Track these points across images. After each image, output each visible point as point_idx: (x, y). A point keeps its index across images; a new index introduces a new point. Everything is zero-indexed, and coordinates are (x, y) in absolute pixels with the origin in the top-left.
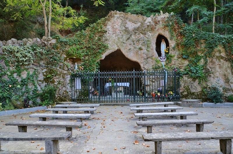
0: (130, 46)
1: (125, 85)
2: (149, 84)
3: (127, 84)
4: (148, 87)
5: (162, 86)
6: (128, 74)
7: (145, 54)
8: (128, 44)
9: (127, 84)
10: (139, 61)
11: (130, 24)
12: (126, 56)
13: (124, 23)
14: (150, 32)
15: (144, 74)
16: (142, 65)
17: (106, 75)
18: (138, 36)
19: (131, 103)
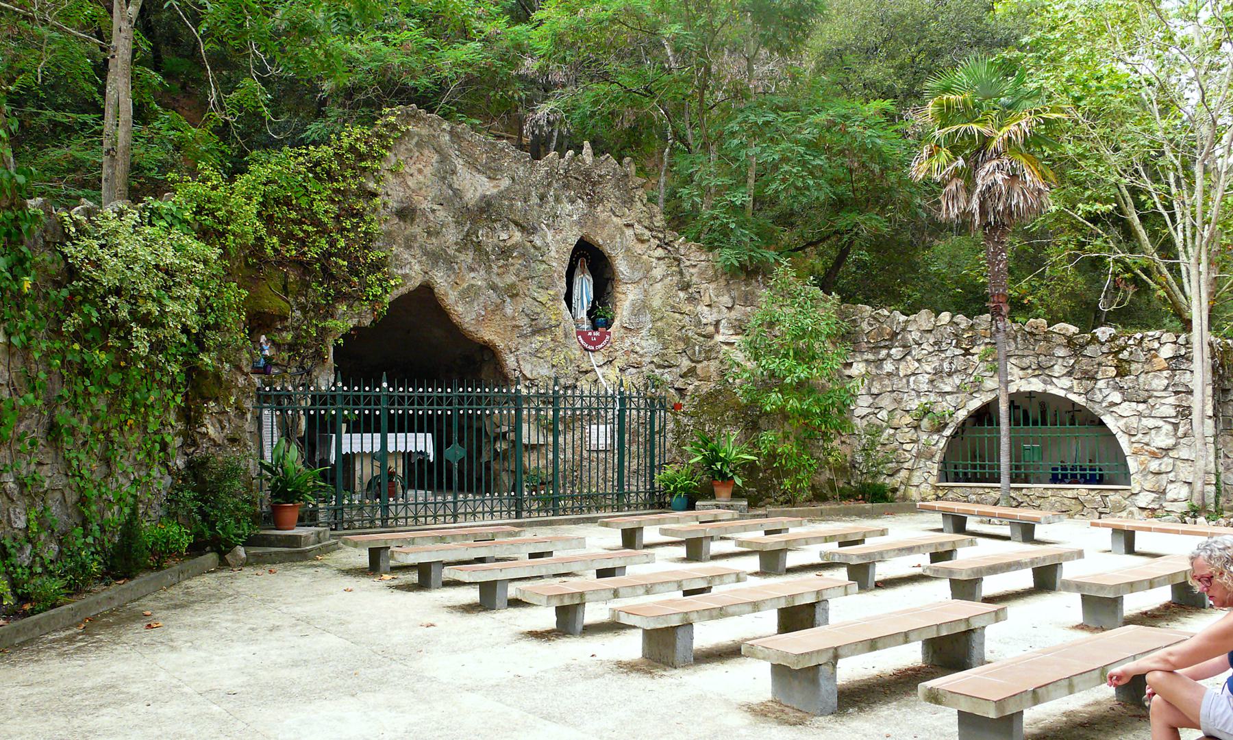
0: (472, 275)
1: (411, 448)
2: (534, 441)
3: (422, 443)
4: (534, 456)
5: (590, 451)
6: (422, 398)
7: (527, 315)
8: (464, 265)
9: (422, 443)
10: (500, 344)
11: (469, 176)
12: (456, 319)
13: (445, 173)
14: (547, 225)
15: (517, 400)
16: (510, 361)
17: (412, 404)
18: (504, 236)
19: (543, 517)
